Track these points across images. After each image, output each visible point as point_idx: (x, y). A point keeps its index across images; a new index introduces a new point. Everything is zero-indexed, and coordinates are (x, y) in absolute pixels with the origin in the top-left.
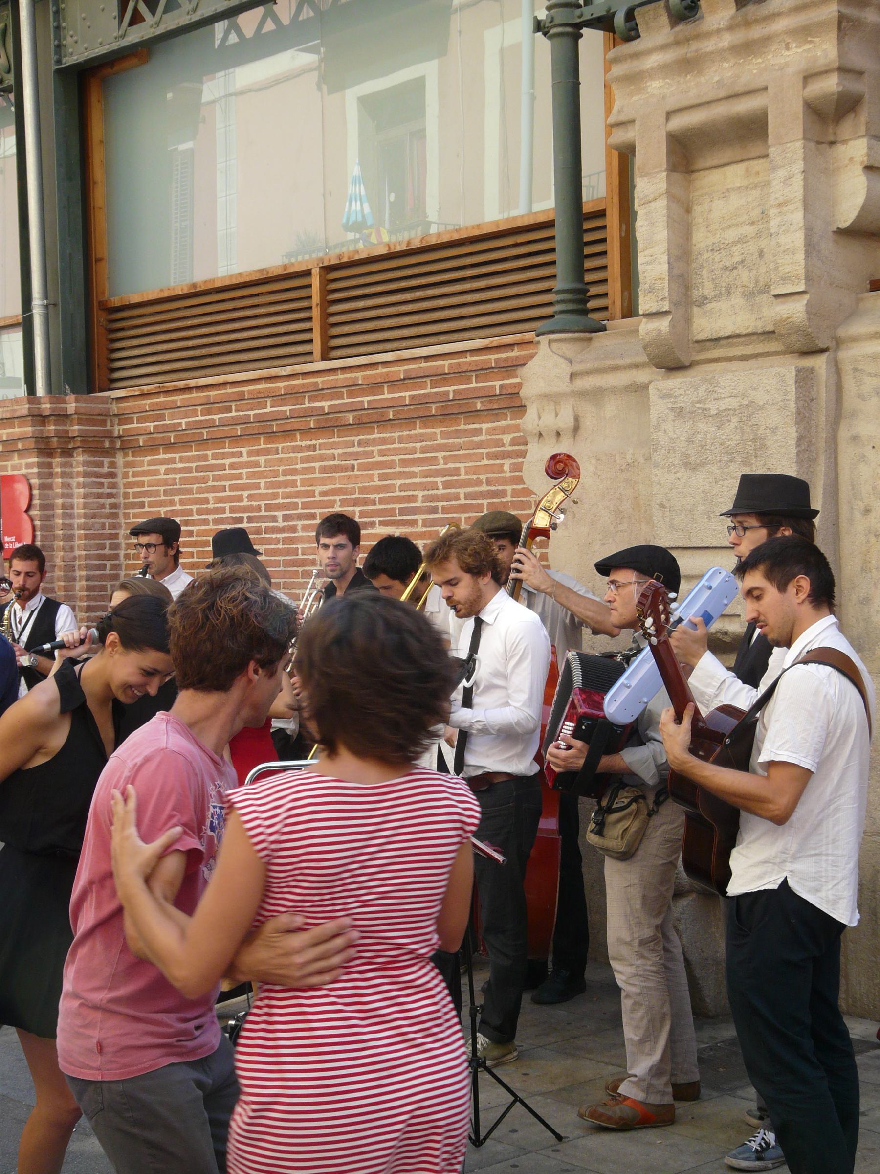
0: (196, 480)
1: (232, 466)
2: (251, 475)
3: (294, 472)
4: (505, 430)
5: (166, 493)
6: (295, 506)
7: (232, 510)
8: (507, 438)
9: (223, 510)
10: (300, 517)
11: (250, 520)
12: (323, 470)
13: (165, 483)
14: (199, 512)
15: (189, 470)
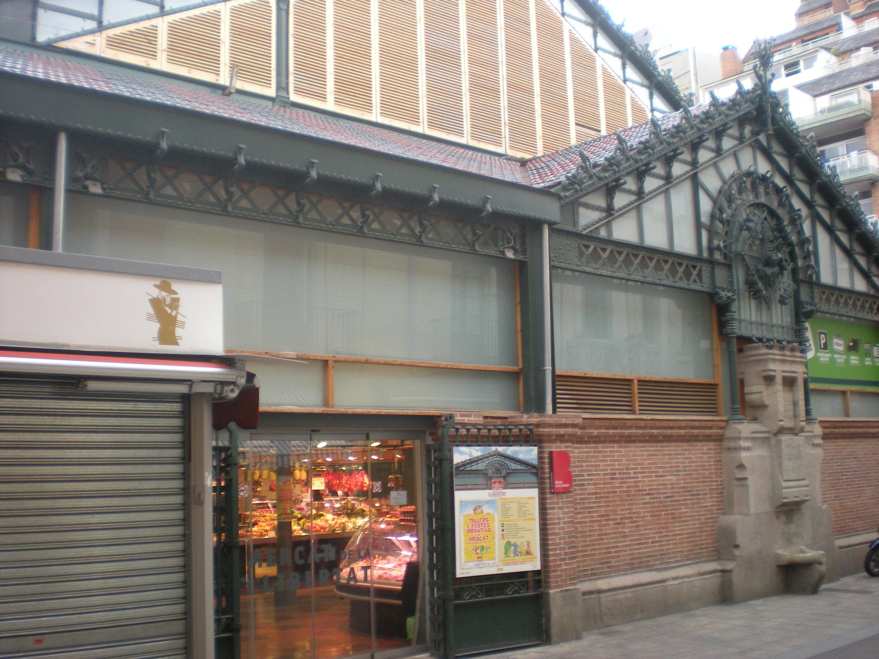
0: (594, 457)
1: (610, 452)
2: (619, 456)
3: (637, 455)
4: (705, 446)
5: (579, 461)
6: (637, 468)
7: (611, 470)
8: (705, 448)
9: (607, 470)
10: (640, 473)
11: (619, 474)
12: (649, 455)
13: (579, 457)
14: (596, 470)
15: (590, 452)
